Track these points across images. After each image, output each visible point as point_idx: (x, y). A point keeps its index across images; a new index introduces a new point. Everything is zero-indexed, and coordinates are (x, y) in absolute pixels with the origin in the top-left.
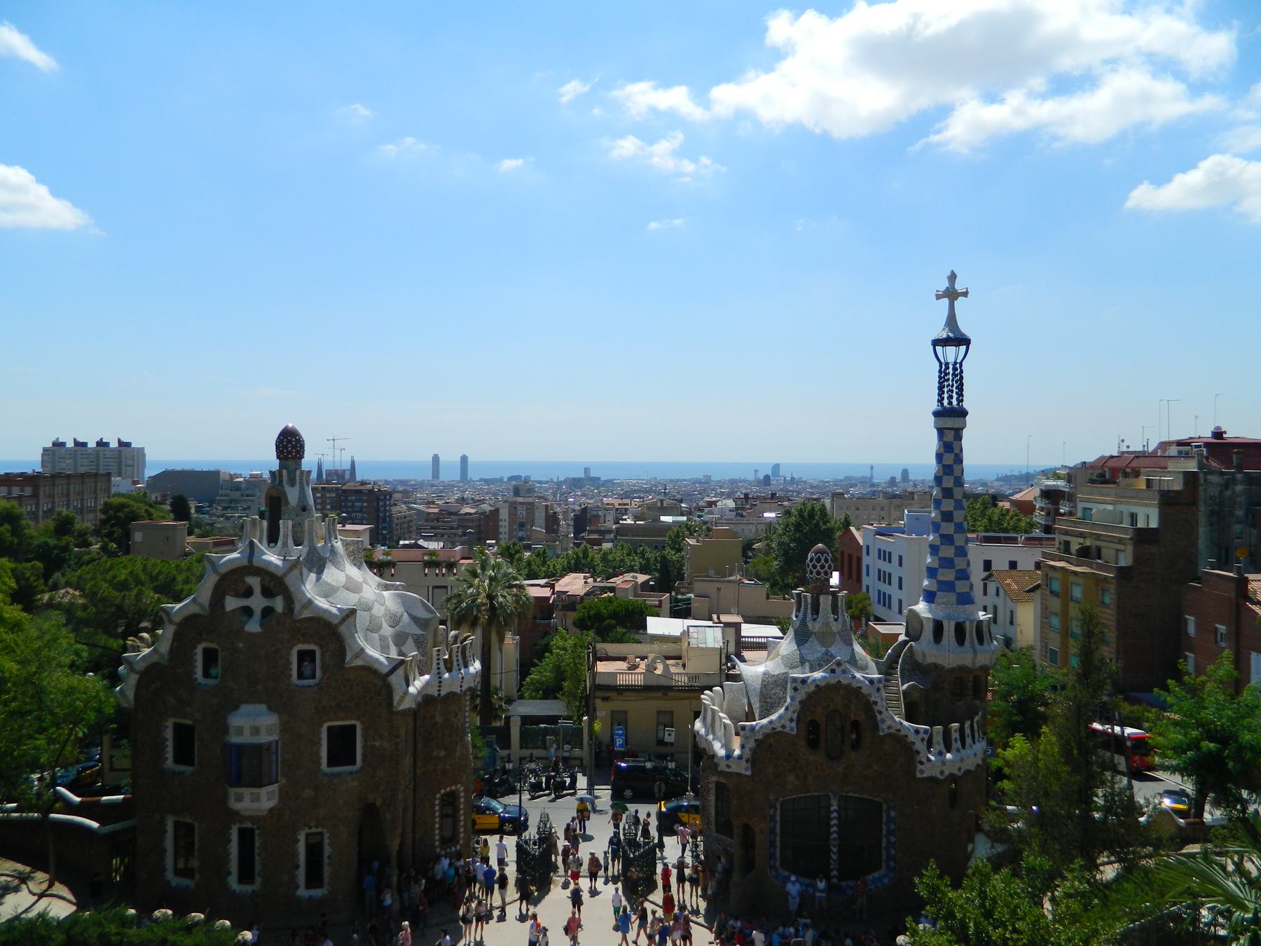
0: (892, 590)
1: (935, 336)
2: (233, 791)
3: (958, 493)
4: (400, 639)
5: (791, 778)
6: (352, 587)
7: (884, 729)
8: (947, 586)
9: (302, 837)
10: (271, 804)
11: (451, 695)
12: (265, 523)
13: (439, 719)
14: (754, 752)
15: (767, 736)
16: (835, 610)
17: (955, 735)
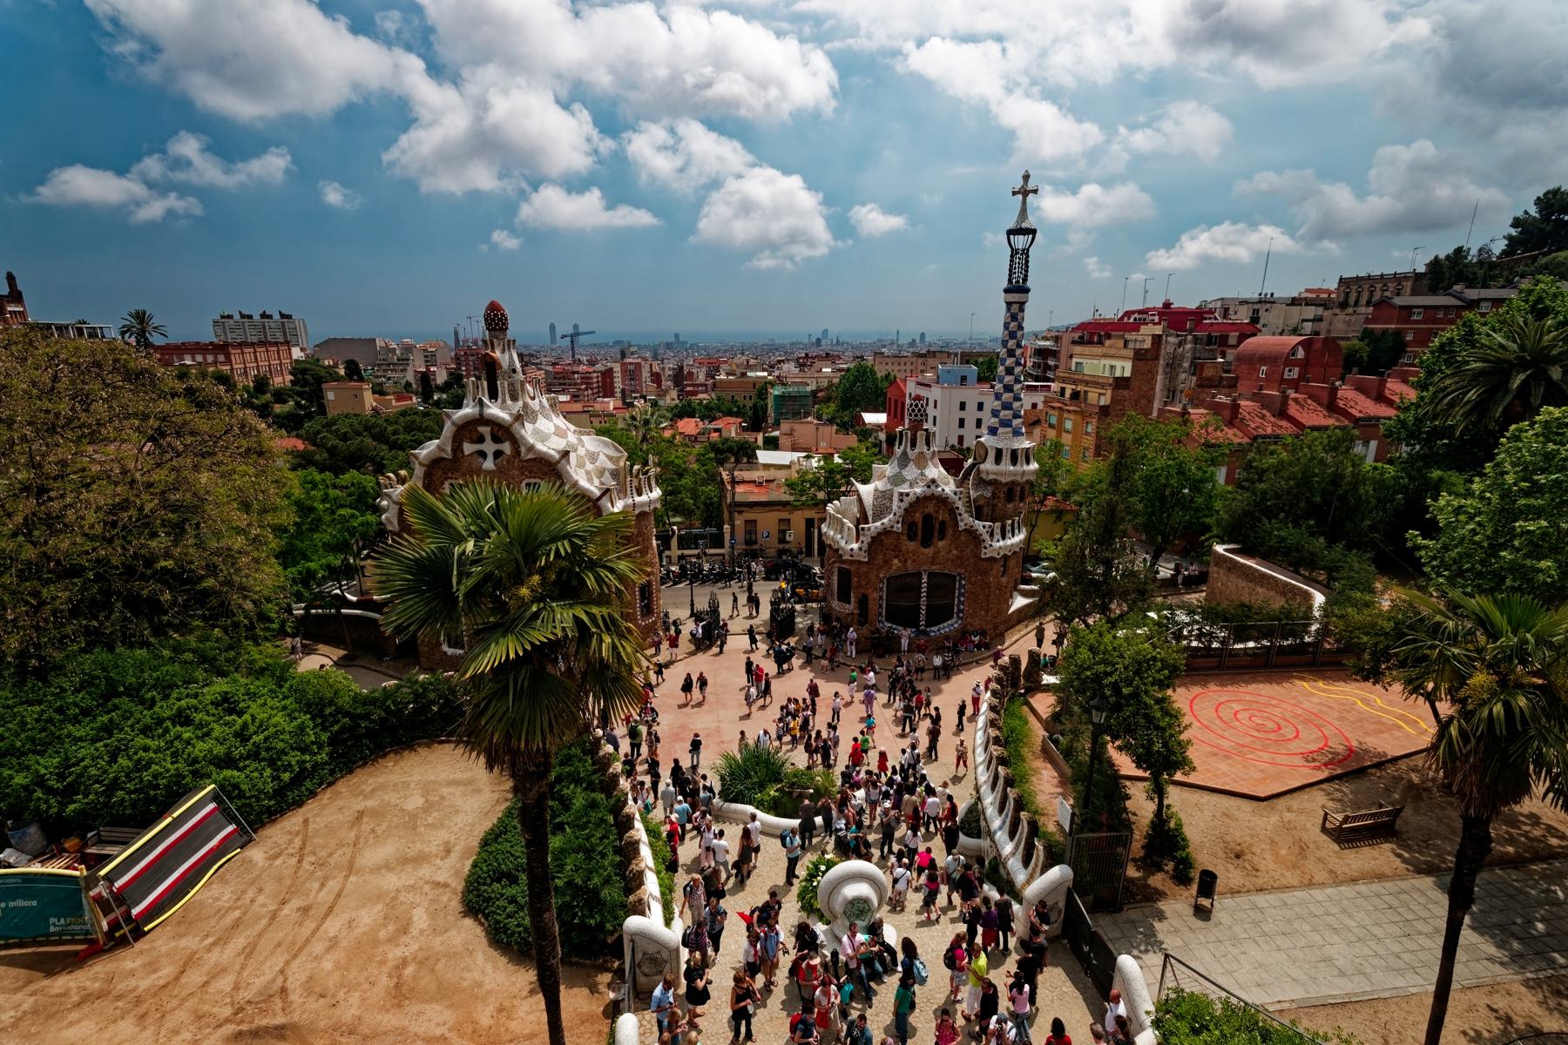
1: (1011, 224)
4: (601, 473)
5: (896, 561)
7: (962, 526)
14: (870, 545)
15: (879, 534)
16: (928, 444)
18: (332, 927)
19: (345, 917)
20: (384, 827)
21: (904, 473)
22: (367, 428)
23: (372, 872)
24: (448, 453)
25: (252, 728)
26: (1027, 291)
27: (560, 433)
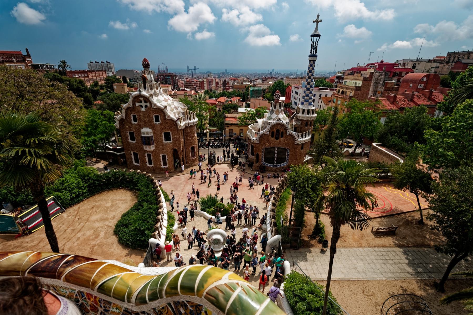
0: (297, 101)
1: (312, 33)
2: (144, 146)
3: (312, 77)
4: (179, 113)
5: (267, 144)
6: (166, 100)
8: (306, 101)
9: (161, 156)
10: (154, 149)
11: (191, 126)
12: (142, 85)
13: (189, 131)
14: (259, 138)
15: (262, 135)
16: (280, 107)
17: (304, 135)
18: (79, 235)
19: (83, 233)
20: (99, 210)
21: (272, 116)
22: (118, 98)
23: (93, 222)
24: (131, 106)
25: (65, 181)
26: (316, 56)
27: (166, 100)
